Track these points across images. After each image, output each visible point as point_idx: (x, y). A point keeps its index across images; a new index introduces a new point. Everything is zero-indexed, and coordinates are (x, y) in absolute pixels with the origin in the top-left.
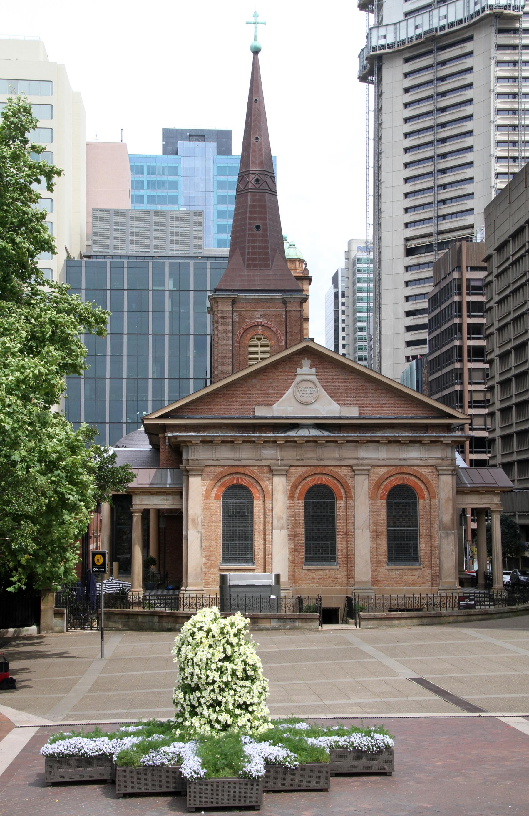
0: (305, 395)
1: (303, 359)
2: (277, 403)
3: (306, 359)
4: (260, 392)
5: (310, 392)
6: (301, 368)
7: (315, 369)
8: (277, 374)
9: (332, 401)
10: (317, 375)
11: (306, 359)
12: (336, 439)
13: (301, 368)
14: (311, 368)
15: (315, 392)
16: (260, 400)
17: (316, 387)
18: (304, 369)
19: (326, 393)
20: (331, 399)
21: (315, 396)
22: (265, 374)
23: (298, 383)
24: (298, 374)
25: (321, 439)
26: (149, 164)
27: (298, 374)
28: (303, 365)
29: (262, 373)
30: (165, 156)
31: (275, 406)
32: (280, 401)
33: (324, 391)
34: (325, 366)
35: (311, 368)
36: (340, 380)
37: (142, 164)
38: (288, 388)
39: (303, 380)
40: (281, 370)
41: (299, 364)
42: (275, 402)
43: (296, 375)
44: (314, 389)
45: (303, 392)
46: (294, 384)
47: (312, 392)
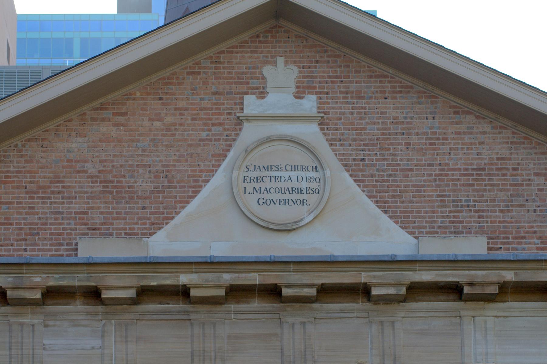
0: (276, 197)
1: (267, 63)
2: (167, 228)
3: (280, 61)
4: (98, 188)
5: (296, 185)
6: (262, 94)
7: (314, 97)
8: (169, 119)
9: (385, 217)
10: (322, 124)
11: (280, 61)
12: (364, 277)
13: (262, 94)
14: (299, 96)
15: (314, 185)
16: (98, 219)
17: (319, 166)
18: (271, 98)
19: (359, 190)
20: (378, 211)
21: (313, 199)
22: (121, 119)
23: (248, 152)
24: (249, 119)
25: (296, 278)
26: (85, 35)
27: (249, 119)
28: (270, 84)
29: (107, 114)
30: (124, 17)
31: (160, 237)
32: (178, 219)
33: (350, 180)
34: (353, 87)
35: (299, 96)
36: (414, 139)
37: (68, 35)
38: (212, 172)
39: (269, 140)
40: (182, 104)
41: (254, 83)
42: (159, 226)
43: (239, 122)
44: (313, 174)
45: (268, 184)
46: (231, 155)
47: (304, 185)
